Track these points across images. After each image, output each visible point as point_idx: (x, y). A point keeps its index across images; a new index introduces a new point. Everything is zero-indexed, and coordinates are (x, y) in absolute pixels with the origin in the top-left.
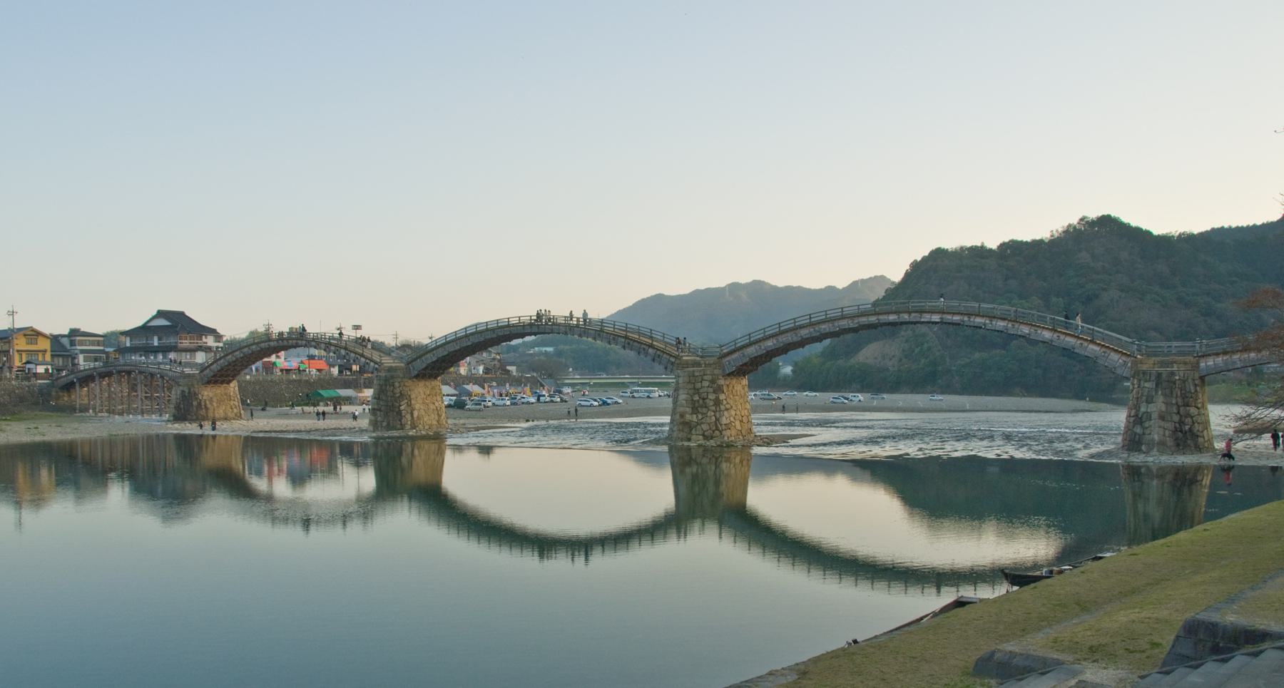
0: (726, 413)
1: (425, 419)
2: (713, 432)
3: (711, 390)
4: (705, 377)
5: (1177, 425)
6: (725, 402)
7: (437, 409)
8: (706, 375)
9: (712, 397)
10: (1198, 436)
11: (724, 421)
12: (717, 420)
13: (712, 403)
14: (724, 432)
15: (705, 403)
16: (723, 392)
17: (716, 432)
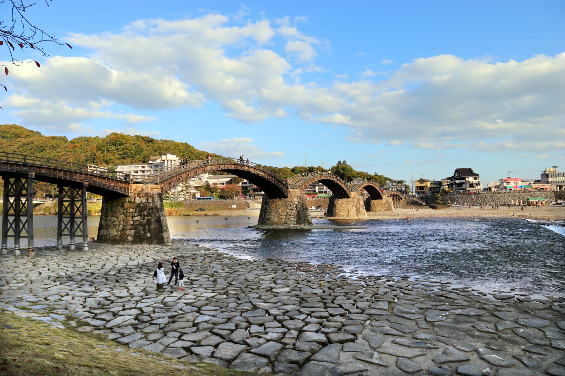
0: (268, 214)
6: (268, 209)
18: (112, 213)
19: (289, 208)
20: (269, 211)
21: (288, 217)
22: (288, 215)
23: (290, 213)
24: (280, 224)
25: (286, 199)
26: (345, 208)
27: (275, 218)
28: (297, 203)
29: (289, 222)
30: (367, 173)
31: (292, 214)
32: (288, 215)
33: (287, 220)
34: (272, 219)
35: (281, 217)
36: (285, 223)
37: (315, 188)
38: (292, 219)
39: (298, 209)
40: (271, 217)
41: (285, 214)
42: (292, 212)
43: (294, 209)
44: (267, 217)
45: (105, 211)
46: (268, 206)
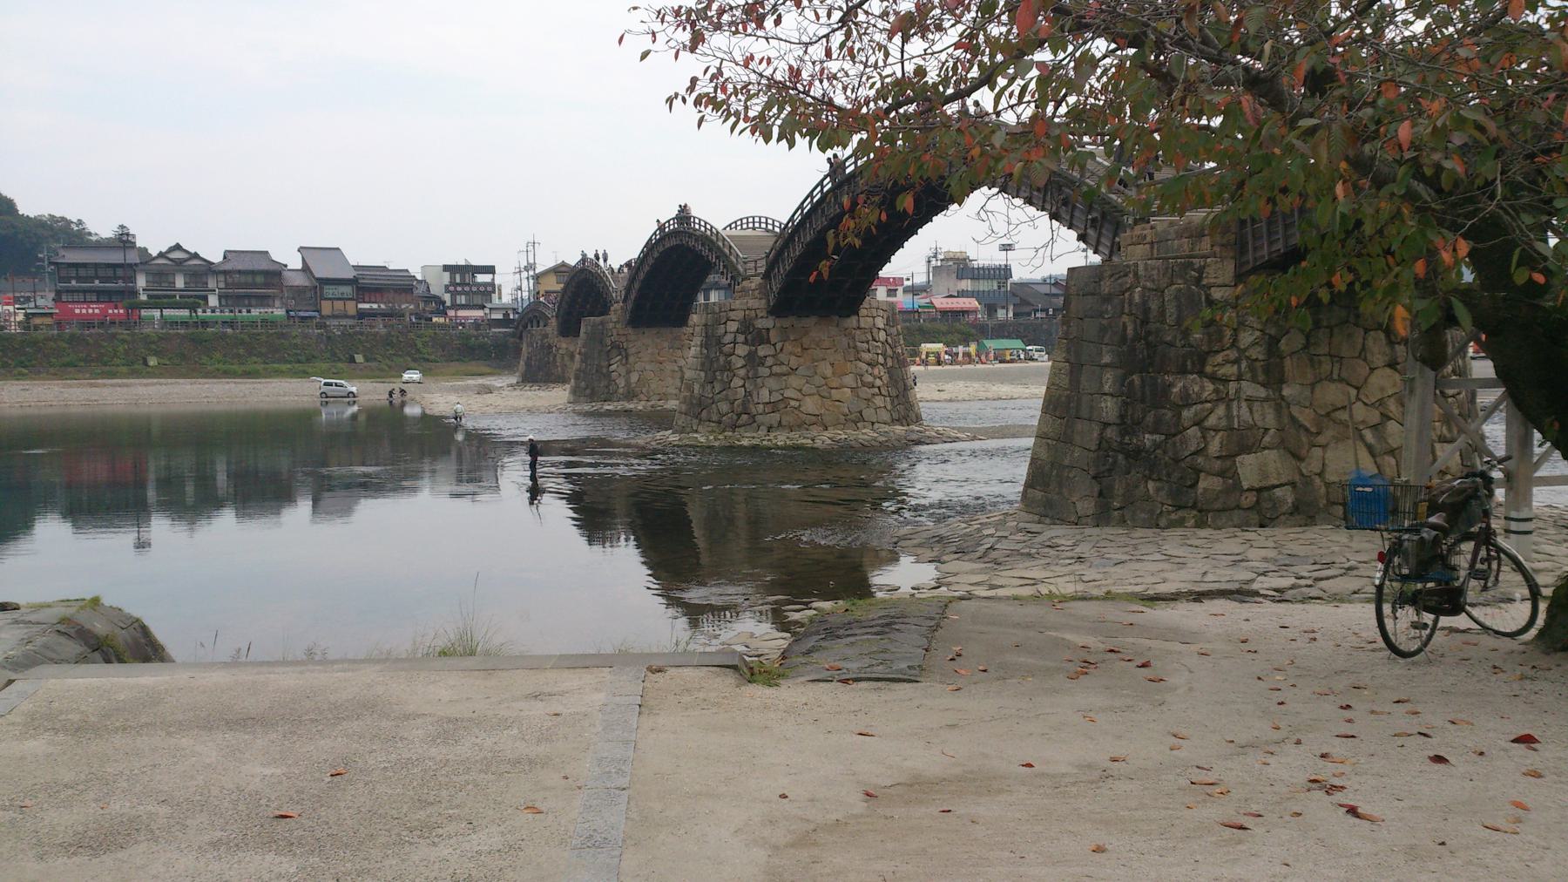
1: (653, 386)
2: (739, 415)
3: (741, 338)
4: (732, 315)
5: (1111, 433)
6: (770, 361)
7: (682, 371)
8: (734, 310)
9: (742, 350)
10: (1198, 471)
11: (765, 395)
12: (748, 394)
13: (741, 363)
14: (759, 418)
15: (730, 363)
16: (768, 342)
17: (745, 417)
18: (1313, 361)
19: (866, 356)
20: (776, 369)
21: (866, 392)
22: (864, 384)
23: (870, 379)
24: (836, 424)
25: (853, 321)
26: (669, 367)
27: (808, 399)
28: (882, 336)
29: (868, 413)
30: (80, 222)
31: (878, 383)
32: (864, 384)
33: (863, 405)
34: (796, 404)
35: (835, 394)
36: (858, 419)
37: (133, 280)
38: (879, 401)
39: (890, 364)
40: (788, 393)
41: (849, 380)
42: (876, 371)
43: (881, 359)
44: (765, 395)
45: (1257, 353)
46: (762, 351)
